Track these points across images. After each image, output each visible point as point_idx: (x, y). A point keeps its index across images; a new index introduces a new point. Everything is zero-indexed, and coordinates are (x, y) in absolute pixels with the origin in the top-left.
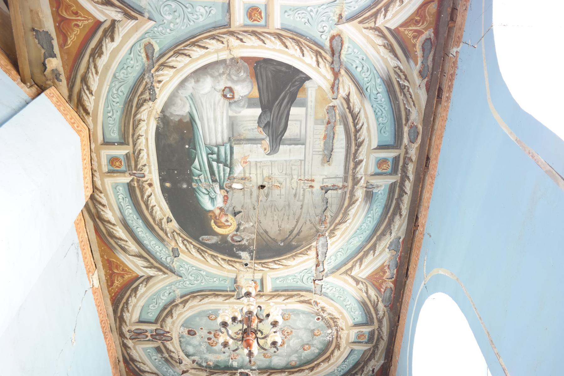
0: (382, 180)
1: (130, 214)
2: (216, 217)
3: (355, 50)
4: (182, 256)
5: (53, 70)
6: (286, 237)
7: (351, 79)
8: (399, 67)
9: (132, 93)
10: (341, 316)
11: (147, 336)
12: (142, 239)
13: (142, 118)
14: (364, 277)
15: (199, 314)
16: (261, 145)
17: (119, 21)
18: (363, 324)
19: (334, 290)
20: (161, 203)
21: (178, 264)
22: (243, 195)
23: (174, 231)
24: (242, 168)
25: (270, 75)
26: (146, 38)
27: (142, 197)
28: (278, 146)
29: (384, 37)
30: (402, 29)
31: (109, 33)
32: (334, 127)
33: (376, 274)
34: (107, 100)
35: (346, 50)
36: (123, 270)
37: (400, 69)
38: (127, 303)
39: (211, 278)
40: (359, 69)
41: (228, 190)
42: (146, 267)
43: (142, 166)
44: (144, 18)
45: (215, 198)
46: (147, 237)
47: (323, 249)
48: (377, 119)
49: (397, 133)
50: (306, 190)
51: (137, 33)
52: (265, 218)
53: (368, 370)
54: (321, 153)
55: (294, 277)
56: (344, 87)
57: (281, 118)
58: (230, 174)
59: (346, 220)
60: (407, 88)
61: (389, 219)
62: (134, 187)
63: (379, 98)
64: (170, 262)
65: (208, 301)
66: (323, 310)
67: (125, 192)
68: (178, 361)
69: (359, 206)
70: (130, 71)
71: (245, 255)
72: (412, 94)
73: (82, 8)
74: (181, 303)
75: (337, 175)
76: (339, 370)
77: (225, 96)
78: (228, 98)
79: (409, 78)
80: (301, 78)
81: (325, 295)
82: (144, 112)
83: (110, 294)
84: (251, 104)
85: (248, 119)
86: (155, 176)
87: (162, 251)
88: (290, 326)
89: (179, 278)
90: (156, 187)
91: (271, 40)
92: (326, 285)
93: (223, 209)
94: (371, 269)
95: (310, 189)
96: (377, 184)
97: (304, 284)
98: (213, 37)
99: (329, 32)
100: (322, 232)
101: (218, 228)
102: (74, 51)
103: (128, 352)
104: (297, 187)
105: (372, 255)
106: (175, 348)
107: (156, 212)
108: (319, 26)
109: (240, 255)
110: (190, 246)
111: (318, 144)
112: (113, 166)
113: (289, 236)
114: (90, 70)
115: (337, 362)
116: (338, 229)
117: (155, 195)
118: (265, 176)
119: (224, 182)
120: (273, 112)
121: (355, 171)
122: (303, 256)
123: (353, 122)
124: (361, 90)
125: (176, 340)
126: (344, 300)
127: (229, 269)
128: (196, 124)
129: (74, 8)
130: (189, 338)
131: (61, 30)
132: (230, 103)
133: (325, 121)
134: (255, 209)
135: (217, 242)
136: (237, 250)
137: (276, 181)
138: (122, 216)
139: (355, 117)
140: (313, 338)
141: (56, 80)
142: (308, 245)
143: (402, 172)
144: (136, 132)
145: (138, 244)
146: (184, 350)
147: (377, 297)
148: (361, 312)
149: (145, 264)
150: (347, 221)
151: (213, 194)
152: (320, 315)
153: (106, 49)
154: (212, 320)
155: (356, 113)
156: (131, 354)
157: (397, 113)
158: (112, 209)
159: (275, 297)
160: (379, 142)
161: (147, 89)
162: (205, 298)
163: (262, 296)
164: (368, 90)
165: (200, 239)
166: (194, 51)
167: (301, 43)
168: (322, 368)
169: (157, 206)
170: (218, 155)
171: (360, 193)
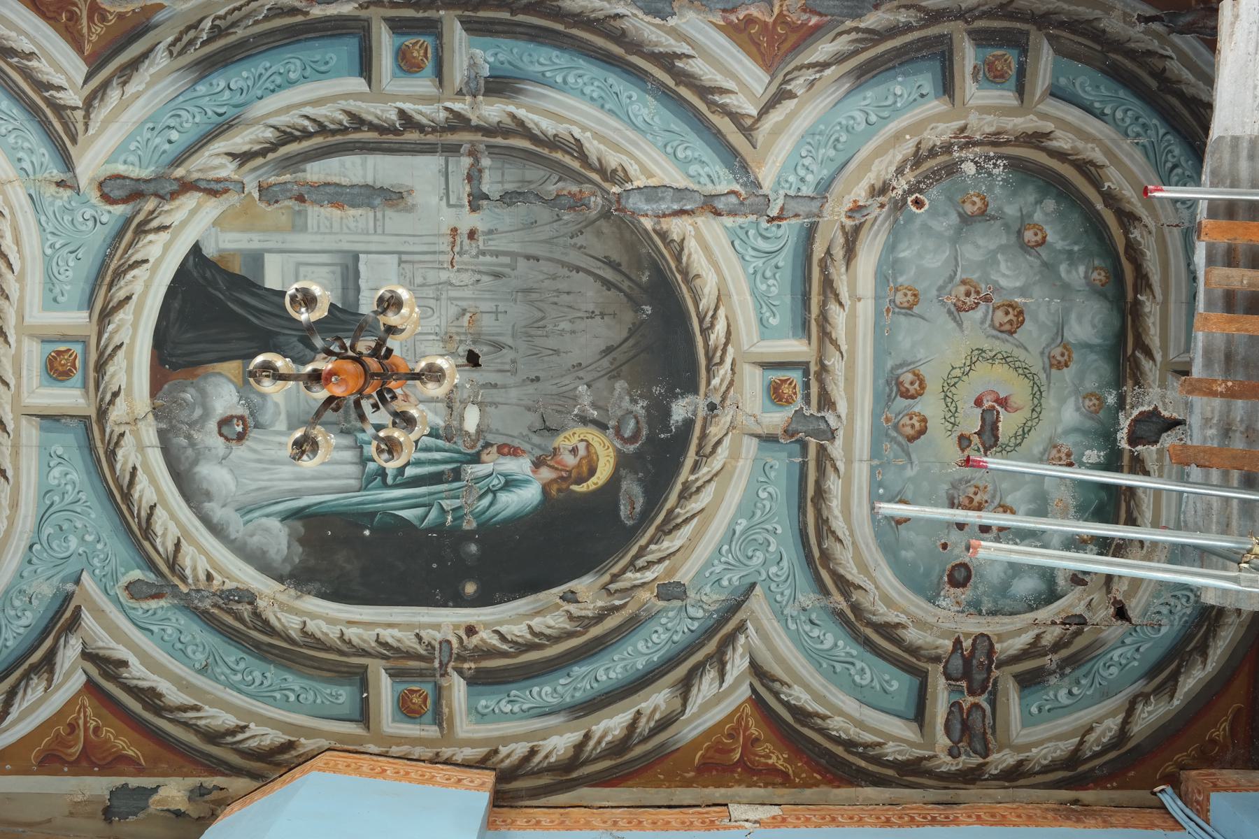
1: (555, 690)
2: (562, 478)
3: (132, 148)
5: (190, 799)
6: (625, 300)
7: (196, 151)
8: (170, 45)
10: (908, 137)
11: (976, 706)
12: (631, 672)
14: (767, 79)
17: (84, 643)
19: (807, 161)
21: (707, 589)
23: (604, 587)
25: (189, 335)
27: (504, 654)
29: (105, 86)
30: (88, 48)
33: (757, 45)
34: (260, 699)
35: (131, 168)
36: (730, 736)
37: (173, 44)
38: (850, 745)
39: (759, 505)
40: (174, 135)
42: (722, 675)
43: (420, 643)
45: (505, 476)
46: (624, 659)
47: (663, 199)
48: (292, 83)
49: (329, 33)
50: (481, 247)
52: (566, 353)
53: (1147, 38)
54: (379, 215)
55: (759, 276)
56: (215, 168)
59: (573, 141)
60: (217, 22)
61: (575, 25)
62: (478, 670)
63: (241, 83)
64: (703, 609)
65: (841, 519)
66: (884, 189)
67: (493, 693)
68: (1074, 628)
69: (531, 109)
71: (680, 410)
72: (231, 7)
73: (60, 714)
74: (846, 595)
76: (1138, 129)
77: (241, 437)
79: (194, 20)
80: (196, 265)
81: (824, 189)
83: (816, 784)
86: (447, 616)
87: (669, 625)
88: (940, 289)
89: (758, 590)
90: (476, 618)
91: (116, 331)
92: (787, 185)
93: (538, 458)
94: (740, 62)
95: (481, 239)
96: (465, 66)
98: (111, 455)
99: (94, 206)
100: (610, 202)
101: (598, 474)
103: (1037, 768)
105: (690, 61)
106: (1020, 632)
107: (549, 627)
108: (84, 228)
109: (680, 424)
110: (653, 552)
111: (357, 221)
113: (621, 290)
114: (191, 722)
115: (1101, 137)
116: (599, 160)
117: (501, 623)
119: (459, 452)
120: (278, 330)
121: (430, 126)
122: (686, 252)
125: (991, 626)
126: (848, 130)
127: (726, 453)
128: (309, 507)
129: (62, 729)
130: (980, 586)
132: (255, 427)
133: (297, 208)
134: (538, 379)
135: (639, 480)
136: (667, 428)
137: (455, 323)
138: (562, 713)
139: (286, 137)
140: (993, 218)
141: (207, 798)
142: (651, 239)
143: (432, 9)
145: (648, 685)
146: (1030, 605)
147: (840, 34)
148: (895, 78)
149: (711, 676)
150: (577, 136)
151: (495, 482)
152: (904, 200)
153: (144, 679)
155: (278, 134)
156: (1045, 762)
158: (545, 734)
159: (829, 329)
160: (350, 75)
163: (823, 368)
164: (221, 110)
165: (630, 523)
166: (141, 498)
168: (1126, 185)
169: (532, 623)
171: (493, 111)
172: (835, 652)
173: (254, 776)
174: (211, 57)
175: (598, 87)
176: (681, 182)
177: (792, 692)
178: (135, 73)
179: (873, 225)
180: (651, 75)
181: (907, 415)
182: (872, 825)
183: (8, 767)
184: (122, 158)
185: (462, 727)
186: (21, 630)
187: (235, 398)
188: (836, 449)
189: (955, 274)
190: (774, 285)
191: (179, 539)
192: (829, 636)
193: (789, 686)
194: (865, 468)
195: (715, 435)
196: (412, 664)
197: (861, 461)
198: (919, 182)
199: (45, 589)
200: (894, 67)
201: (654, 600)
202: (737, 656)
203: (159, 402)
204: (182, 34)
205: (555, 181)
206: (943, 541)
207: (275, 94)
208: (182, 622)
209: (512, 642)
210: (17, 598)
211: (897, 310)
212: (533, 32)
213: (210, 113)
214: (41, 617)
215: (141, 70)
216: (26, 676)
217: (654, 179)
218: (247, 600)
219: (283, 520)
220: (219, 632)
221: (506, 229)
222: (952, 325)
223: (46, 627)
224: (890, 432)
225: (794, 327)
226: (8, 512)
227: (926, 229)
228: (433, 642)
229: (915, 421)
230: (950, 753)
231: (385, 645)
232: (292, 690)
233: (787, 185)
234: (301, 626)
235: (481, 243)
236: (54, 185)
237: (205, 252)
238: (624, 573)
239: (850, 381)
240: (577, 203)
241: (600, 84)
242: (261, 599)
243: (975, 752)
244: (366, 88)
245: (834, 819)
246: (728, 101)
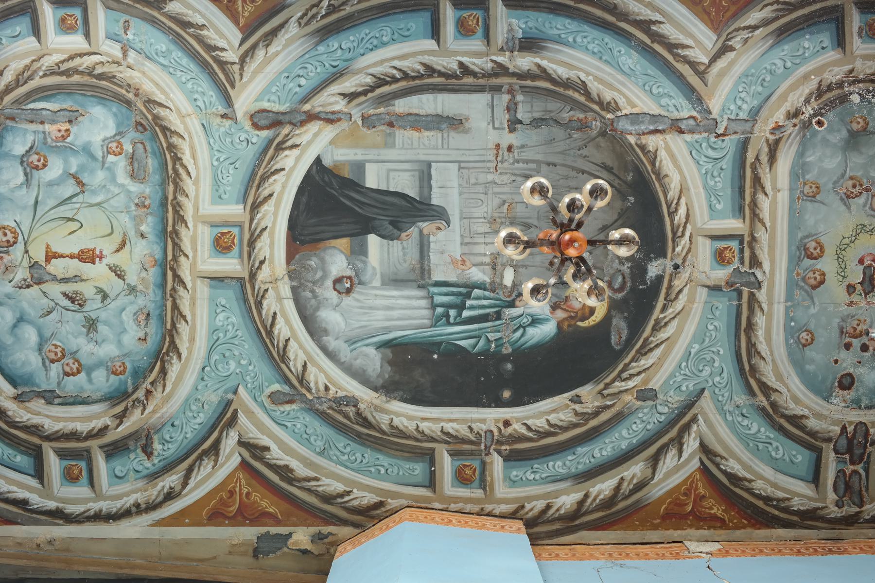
0: (499, 25)
1: (564, 464)
2: (571, 317)
3: (274, 90)
4: (656, 383)
7: (318, 93)
8: (299, 19)
10: (813, 77)
11: (855, 472)
12: (617, 451)
13: (388, 422)
14: (715, 38)
15: (798, 364)
16: (431, 236)
17: (240, 435)
18: (838, 29)
19: (743, 95)
20: (542, 409)
21: (672, 393)
22: (526, 268)
23: (600, 393)
24: (474, 269)
25: (313, 221)
27: (530, 440)
28: (434, 208)
29: (254, 47)
30: (242, 21)
32: (400, 116)
33: (708, 14)
35: (273, 104)
36: (685, 494)
37: (302, 18)
38: (767, 499)
39: (708, 334)
40: (303, 81)
41: (515, 293)
43: (471, 432)
45: (532, 316)
46: (612, 442)
47: (642, 122)
48: (384, 44)
49: (410, 9)
50: (516, 157)
54: (445, 135)
55: (709, 176)
56: (331, 104)
57: (384, 203)
58: (485, 289)
59: (580, 82)
62: (511, 450)
63: (349, 45)
64: (668, 407)
65: (764, 343)
66: (797, 113)
67: (521, 466)
69: (551, 60)
71: (653, 269)
74: (767, 396)
75: (487, 104)
77: (349, 291)
78: (352, 285)
80: (318, 172)
81: (755, 113)
83: (744, 527)
84: (361, 251)
85: (386, 255)
86: (490, 413)
87: (644, 418)
88: (835, 183)
89: (706, 393)
91: (262, 219)
92: (729, 112)
93: (555, 304)
94: (696, 26)
95: (516, 151)
97: (728, 157)
98: (259, 304)
99: (247, 132)
100: (606, 125)
102: (285, 506)
104: (511, 174)
105: (661, 26)
109: (653, 278)
110: (633, 368)
111: (430, 140)
116: (598, 96)
117: (528, 418)
118: (490, 230)
119: (500, 300)
120: (375, 216)
121: (481, 73)
122: (658, 159)
123: (391, 85)
124: (336, 76)
127: (685, 299)
128: (395, 339)
132: (359, 284)
133: (388, 132)
135: (625, 318)
136: (644, 282)
137: (498, 210)
138: (569, 480)
139: (381, 82)
141: (326, 540)
142: (634, 150)
144: (412, 435)
145: (629, 460)
147: (766, 6)
148: (804, 36)
150: (583, 79)
151: (525, 320)
153: (281, 460)
154: (813, 340)
155: (375, 80)
157: (374, 13)
158: (557, 494)
159: (758, 211)
160: (425, 38)
162: (756, 350)
163: (753, 239)
164: (335, 64)
165: (618, 348)
166: (279, 334)
167: (265, 173)
169: (549, 418)
170: (449, 306)
171: (525, 62)
172: (759, 435)
174: (327, 26)
175: (597, 44)
176: (656, 111)
177: (729, 464)
178: (275, 38)
179: (788, 138)
180: (634, 35)
181: (812, 271)
182: (789, 554)
183: (187, 521)
184: (267, 98)
185: (499, 490)
186: (197, 427)
187: (345, 264)
188: (762, 295)
189: (846, 173)
190: (719, 181)
191: (305, 362)
192: (754, 424)
193: (727, 460)
194: (782, 308)
195: (678, 286)
197: (779, 303)
198: (821, 109)
199: (213, 398)
200: (803, 28)
201: (634, 401)
202: (691, 439)
203: (293, 267)
204: (307, 10)
205: (568, 110)
206: (835, 358)
207: (373, 52)
208: (308, 420)
209: (535, 431)
211: (805, 198)
212: (552, 6)
213: (327, 65)
214: (210, 418)
215: (279, 36)
216: (200, 458)
217: (637, 109)
218: (352, 404)
219: (377, 348)
220: (333, 426)
221: (532, 145)
222: (843, 208)
224: (799, 282)
225: (733, 211)
226: (188, 345)
227: (825, 142)
228: (480, 432)
229: (817, 275)
230: (837, 505)
231: (448, 434)
233: (729, 112)
235: (516, 154)
236: (220, 117)
237: (324, 163)
238: (614, 383)
239: (772, 247)
240: (583, 126)
241: (599, 43)
242: (362, 403)
243: (854, 504)
244: (436, 47)
245: (761, 551)
246: (688, 53)
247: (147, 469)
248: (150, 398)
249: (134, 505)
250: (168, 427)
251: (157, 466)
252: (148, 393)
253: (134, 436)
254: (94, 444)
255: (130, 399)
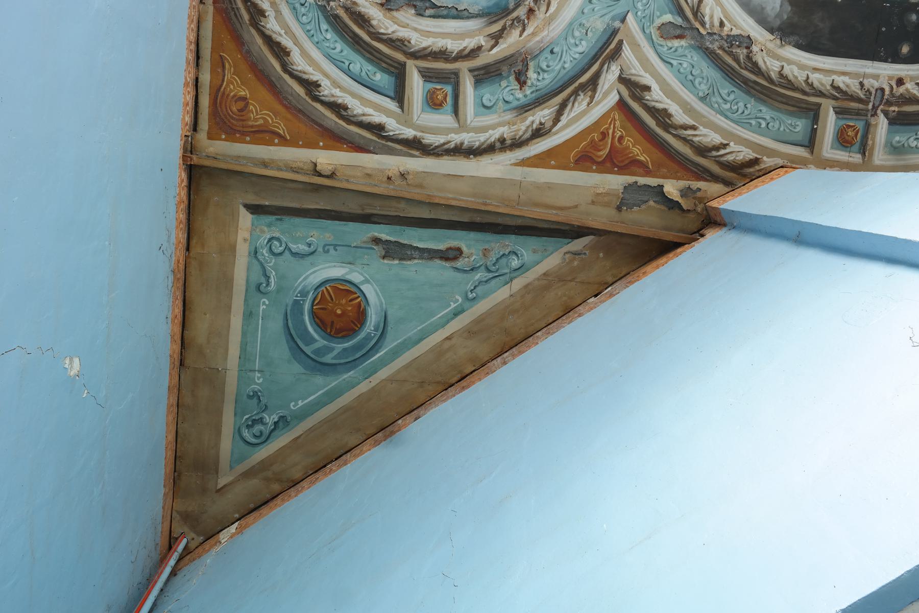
5: (681, 196)
9: (734, 78)
17: (622, 70)
26: (651, 33)
31: (637, 91)
43: (861, 89)
44: (621, 29)
51: (642, 46)
70: (698, 72)
73: (597, 124)
82: (768, 63)
86: (885, 69)
90: (906, 73)
102: (658, 155)
112: (854, 142)
114: (688, 138)
129: (596, 136)
131: (624, 166)
153: (660, 102)
161: (730, 50)
173: (726, 183)
185: (878, 155)
186: (577, 56)
196: (854, 105)
199: (598, 24)
208: (696, 59)
210: (577, 29)
214: (593, 47)
216: (575, 93)
218: (745, 45)
220: (721, 70)
223: (596, 54)
228: (871, 89)
231: (837, 88)
232: (764, 119)
234: (780, 69)
242: (755, 45)
247: (518, 100)
248: (532, 17)
249: (499, 140)
250: (546, 54)
251: (528, 98)
252: (531, 11)
253: (507, 60)
254: (463, 66)
255: (510, 17)
